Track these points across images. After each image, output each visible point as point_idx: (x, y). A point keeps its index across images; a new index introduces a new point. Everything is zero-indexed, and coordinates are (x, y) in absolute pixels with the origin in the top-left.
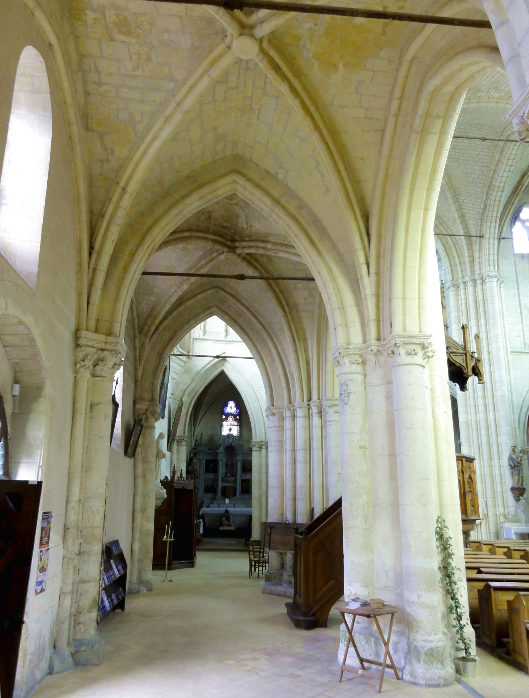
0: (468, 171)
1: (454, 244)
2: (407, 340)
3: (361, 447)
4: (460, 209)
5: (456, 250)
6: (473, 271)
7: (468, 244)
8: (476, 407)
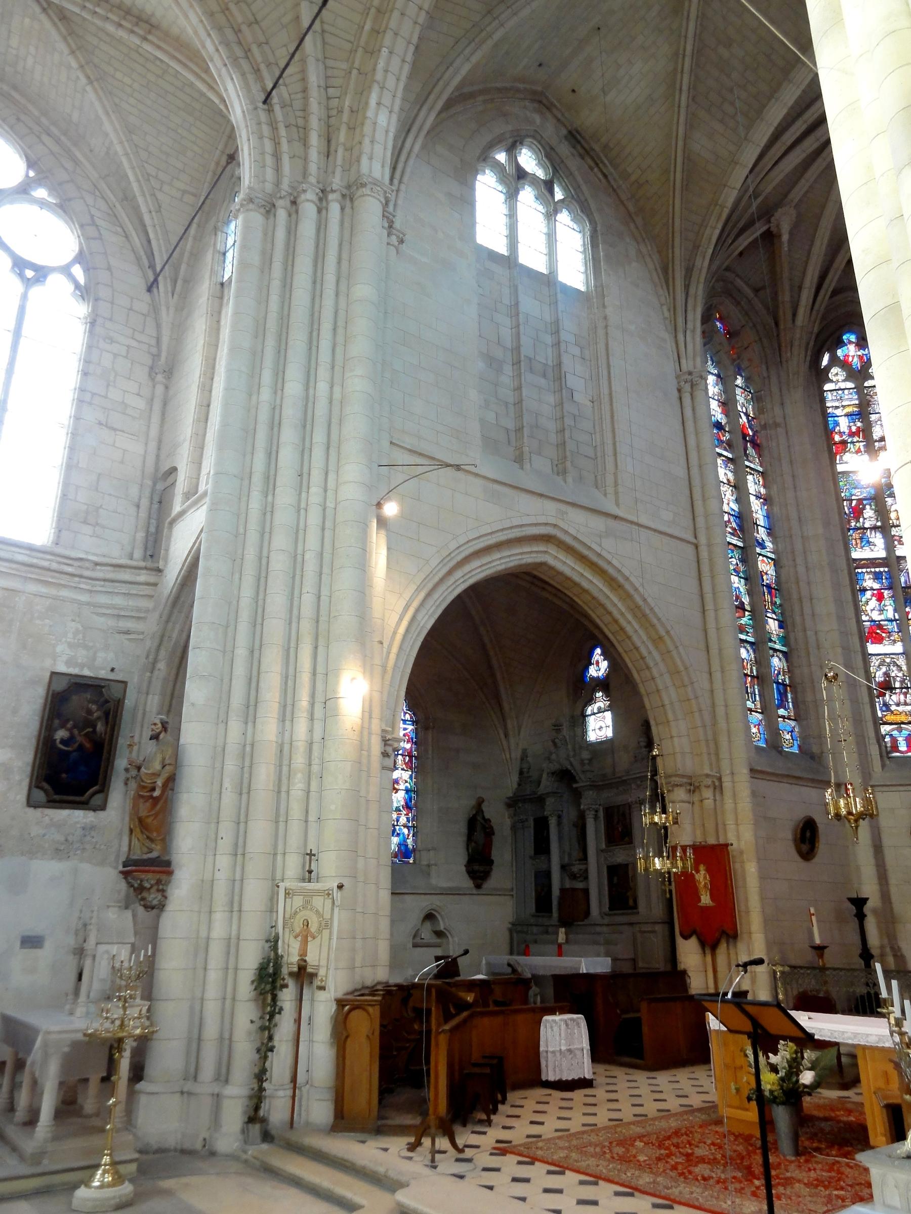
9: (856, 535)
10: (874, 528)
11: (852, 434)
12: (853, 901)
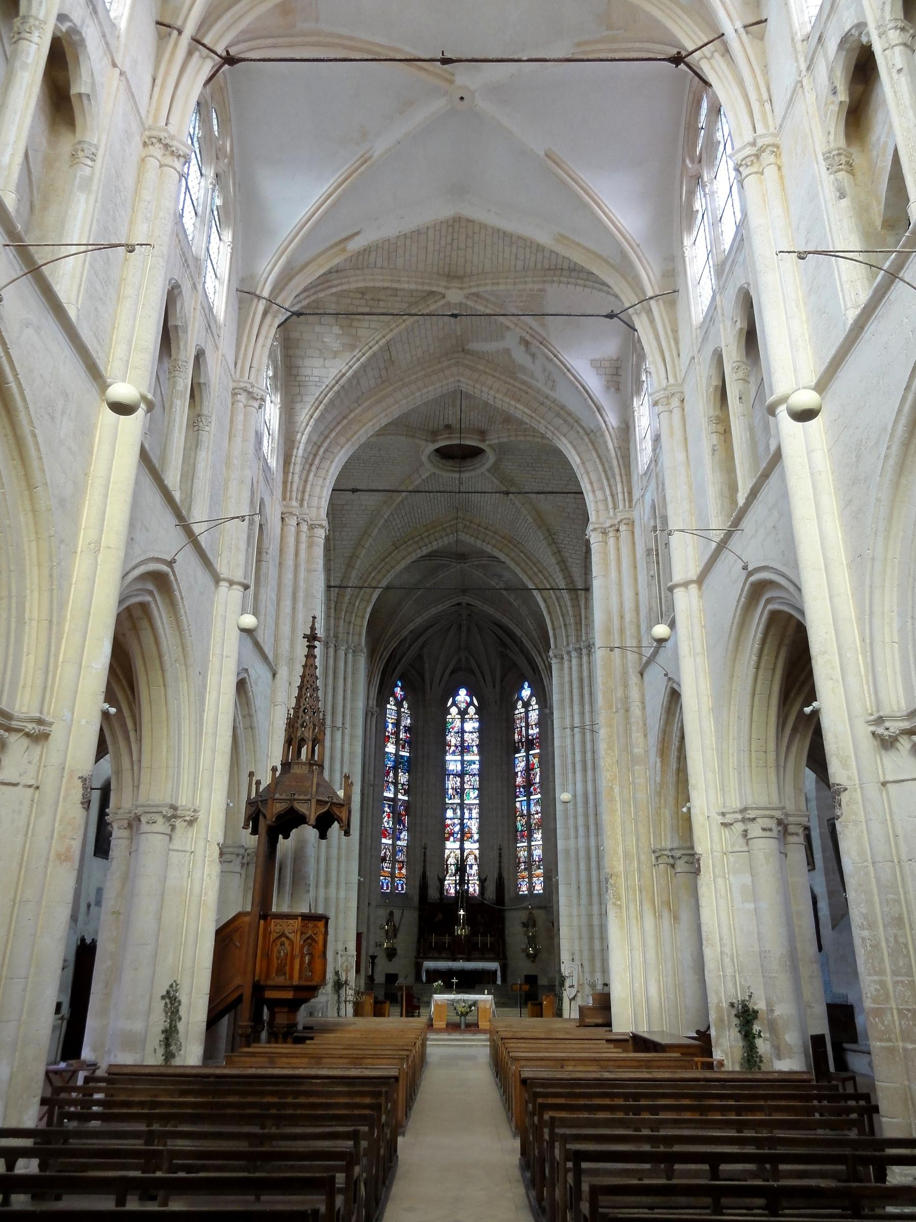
0: (559, 504)
2: (147, 809)
3: (113, 913)
4: (558, 552)
6: (578, 638)
7: (572, 599)
10: (392, 782)
11: (392, 734)
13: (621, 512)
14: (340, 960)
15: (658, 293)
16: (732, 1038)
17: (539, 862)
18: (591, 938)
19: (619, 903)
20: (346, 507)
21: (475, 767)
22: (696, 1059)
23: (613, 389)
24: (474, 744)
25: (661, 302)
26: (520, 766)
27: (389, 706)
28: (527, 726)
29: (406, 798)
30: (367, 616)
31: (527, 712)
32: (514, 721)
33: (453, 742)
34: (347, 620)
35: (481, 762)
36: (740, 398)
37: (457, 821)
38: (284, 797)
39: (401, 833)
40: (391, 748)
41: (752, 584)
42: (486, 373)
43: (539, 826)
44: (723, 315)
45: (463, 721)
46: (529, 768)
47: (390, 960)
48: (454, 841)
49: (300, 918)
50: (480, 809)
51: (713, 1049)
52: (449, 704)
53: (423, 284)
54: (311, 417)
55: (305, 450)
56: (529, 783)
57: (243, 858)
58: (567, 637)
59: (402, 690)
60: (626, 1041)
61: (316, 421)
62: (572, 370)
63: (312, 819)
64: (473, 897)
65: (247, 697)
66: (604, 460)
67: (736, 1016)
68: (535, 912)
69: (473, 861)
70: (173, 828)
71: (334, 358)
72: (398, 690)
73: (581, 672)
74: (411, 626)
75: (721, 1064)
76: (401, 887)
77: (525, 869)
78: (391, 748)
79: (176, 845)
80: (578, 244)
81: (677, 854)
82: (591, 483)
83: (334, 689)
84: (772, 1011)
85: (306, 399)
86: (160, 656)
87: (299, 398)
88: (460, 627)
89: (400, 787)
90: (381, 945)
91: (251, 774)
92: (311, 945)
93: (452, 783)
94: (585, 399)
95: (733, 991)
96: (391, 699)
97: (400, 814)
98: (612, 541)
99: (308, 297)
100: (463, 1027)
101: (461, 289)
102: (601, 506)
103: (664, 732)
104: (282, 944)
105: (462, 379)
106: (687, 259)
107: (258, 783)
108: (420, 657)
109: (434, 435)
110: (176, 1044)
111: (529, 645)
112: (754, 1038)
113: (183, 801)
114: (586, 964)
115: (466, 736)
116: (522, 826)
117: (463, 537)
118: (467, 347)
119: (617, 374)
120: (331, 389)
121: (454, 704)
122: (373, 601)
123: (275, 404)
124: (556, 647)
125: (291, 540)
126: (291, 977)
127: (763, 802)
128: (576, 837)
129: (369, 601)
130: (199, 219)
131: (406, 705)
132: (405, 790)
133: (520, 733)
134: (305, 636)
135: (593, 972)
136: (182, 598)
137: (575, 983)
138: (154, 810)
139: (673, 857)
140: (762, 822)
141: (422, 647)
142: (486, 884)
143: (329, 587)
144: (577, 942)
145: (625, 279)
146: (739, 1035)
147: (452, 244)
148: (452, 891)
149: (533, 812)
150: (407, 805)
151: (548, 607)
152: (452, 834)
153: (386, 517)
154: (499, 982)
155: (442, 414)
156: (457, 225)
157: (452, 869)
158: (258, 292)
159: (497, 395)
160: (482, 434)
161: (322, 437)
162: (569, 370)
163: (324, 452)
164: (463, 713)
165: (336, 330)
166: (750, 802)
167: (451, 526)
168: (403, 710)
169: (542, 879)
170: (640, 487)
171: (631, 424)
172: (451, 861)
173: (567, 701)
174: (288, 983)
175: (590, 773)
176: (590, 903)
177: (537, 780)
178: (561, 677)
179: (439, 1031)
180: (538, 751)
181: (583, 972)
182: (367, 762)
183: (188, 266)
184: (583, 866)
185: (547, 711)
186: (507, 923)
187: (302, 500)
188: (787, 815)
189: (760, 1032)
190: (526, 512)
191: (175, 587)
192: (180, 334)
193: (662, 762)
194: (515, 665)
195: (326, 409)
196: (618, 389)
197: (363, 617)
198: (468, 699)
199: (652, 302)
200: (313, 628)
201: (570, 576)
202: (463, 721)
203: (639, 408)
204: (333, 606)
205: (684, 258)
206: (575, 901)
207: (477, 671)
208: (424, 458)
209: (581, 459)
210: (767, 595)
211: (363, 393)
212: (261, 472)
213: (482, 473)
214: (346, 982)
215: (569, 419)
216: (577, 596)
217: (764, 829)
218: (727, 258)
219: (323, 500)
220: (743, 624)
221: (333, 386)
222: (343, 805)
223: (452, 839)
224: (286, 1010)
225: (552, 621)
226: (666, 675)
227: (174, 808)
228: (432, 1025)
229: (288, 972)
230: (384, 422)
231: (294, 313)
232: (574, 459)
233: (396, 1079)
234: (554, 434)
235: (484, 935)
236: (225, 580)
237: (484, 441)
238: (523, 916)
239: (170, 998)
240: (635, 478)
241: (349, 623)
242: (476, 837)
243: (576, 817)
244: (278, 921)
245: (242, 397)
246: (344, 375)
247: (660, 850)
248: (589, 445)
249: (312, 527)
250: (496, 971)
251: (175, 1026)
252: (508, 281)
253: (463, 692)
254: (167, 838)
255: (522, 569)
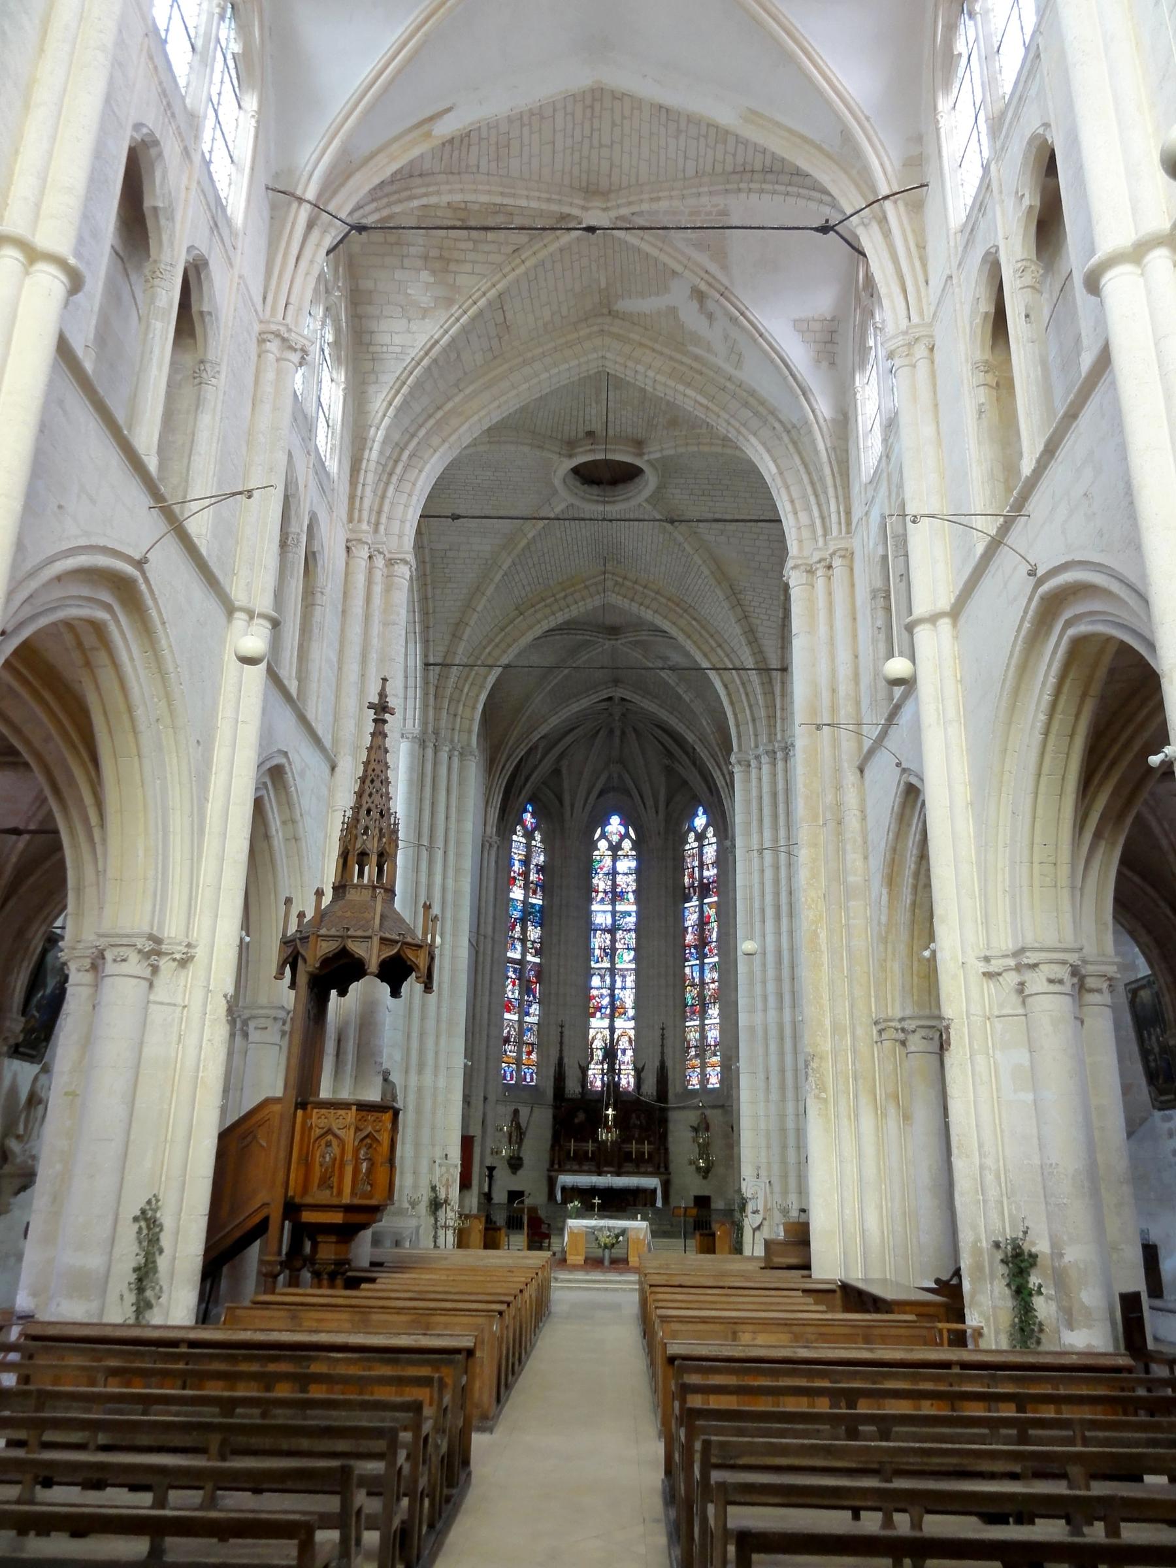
0: (747, 549)
1: (743, 684)
3: (66, 1094)
5: (747, 695)
7: (763, 684)
8: (765, 998)
9: (510, 941)
10: (519, 939)
11: (519, 874)
12: (488, 1168)
13: (836, 538)
14: (438, 1171)
15: (896, 189)
16: (996, 1293)
17: (715, 1046)
18: (784, 1147)
19: (823, 1095)
20: (449, 554)
21: (631, 921)
22: (940, 1325)
23: (825, 364)
24: (630, 889)
25: (900, 204)
26: (691, 919)
27: (515, 838)
28: (701, 866)
29: (537, 960)
30: (480, 707)
31: (701, 847)
32: (683, 859)
33: (602, 887)
34: (452, 712)
35: (638, 913)
36: (1027, 316)
37: (605, 992)
38: (333, 932)
39: (530, 1006)
40: (517, 893)
41: (1042, 598)
42: (641, 345)
43: (715, 999)
44: (1001, 192)
45: (615, 858)
46: (703, 922)
47: (514, 1173)
48: (602, 1018)
49: (354, 1108)
50: (637, 975)
51: (967, 1311)
52: (597, 836)
53: (549, 200)
54: (390, 404)
55: (381, 452)
56: (703, 942)
57: (284, 1024)
58: (756, 735)
59: (533, 816)
60: (833, 1291)
61: (399, 410)
62: (766, 334)
63: (373, 965)
64: (627, 1093)
65: (287, 793)
66: (812, 468)
67: (1002, 1261)
68: (708, 1112)
69: (627, 1045)
70: (155, 970)
71: (423, 318)
72: (528, 818)
73: (774, 783)
74: (544, 729)
75: (978, 1333)
76: (530, 1077)
77: (697, 1056)
78: (517, 893)
79: (160, 994)
80: (778, 124)
81: (910, 1025)
82: (792, 502)
83: (433, 804)
84: (1061, 1255)
85: (383, 378)
86: (130, 709)
87: (373, 377)
88: (611, 732)
89: (529, 945)
90: (498, 1152)
91: (288, 901)
92: (370, 1146)
93: (599, 941)
94: (785, 378)
95: (998, 1224)
96: (518, 828)
97: (529, 981)
98: (820, 583)
99: (377, 210)
100: (607, 1263)
101: (605, 209)
102: (806, 534)
103: (894, 850)
104: (329, 1144)
105: (608, 355)
106: (942, 131)
107: (301, 915)
108: (557, 772)
109: (571, 446)
110: (153, 1289)
111: (704, 754)
112: (1030, 1295)
113: (172, 930)
114: (775, 1181)
115: (620, 879)
116: (693, 998)
117: (615, 599)
118: (615, 308)
119: (831, 342)
120: (419, 364)
121: (603, 836)
122: (489, 686)
123: (337, 384)
124: (740, 746)
125: (360, 579)
126: (340, 1193)
127: (1051, 940)
128: (765, 1010)
129: (482, 687)
130: (198, 57)
131: (538, 836)
132: (536, 949)
133: (691, 876)
134: (371, 706)
135: (785, 1193)
136: (164, 623)
137: (761, 1208)
138: (124, 941)
139: (903, 1030)
140: (1046, 970)
141: (561, 756)
142: (643, 1075)
143: (427, 665)
144: (763, 1153)
145: (846, 172)
146: (1007, 1291)
147: (591, 137)
148: (598, 1083)
149: (707, 980)
150: (539, 970)
151: (729, 695)
152: (599, 1009)
153: (505, 567)
154: (659, 1204)
155: (581, 413)
156: (597, 106)
157: (599, 1055)
158: (299, 193)
159: (658, 377)
160: (639, 445)
161: (407, 436)
162: (761, 335)
163: (410, 457)
164: (615, 848)
165: (425, 276)
166: (1029, 940)
167: (596, 584)
168: (534, 843)
169: (718, 1069)
170: (864, 502)
171: (850, 414)
172: (598, 1044)
173: (755, 823)
174: (335, 1201)
175: (785, 921)
176: (783, 1098)
177: (714, 936)
178: (747, 791)
179: (575, 1268)
180: (715, 899)
181: (772, 1193)
182: (483, 911)
183: (173, 115)
184: (773, 1047)
185: (728, 843)
186: (671, 1126)
187: (377, 524)
188: (1085, 962)
189: (1040, 1286)
190: (700, 562)
191: (150, 603)
192: (163, 222)
193: (889, 894)
194: (685, 783)
195: (410, 393)
196: (833, 364)
197: (474, 708)
198: (622, 830)
199: (888, 204)
200: (382, 694)
201: (761, 652)
202: (615, 858)
203: (863, 388)
204: (432, 691)
205: (938, 130)
206: (761, 1096)
207: (635, 792)
208: (557, 482)
209: (777, 466)
210: (1067, 614)
211: (465, 374)
212: (311, 471)
213: (640, 505)
214: (446, 1201)
215: (761, 409)
216: (771, 679)
217: (1051, 981)
218: (1007, 106)
219: (408, 525)
220: (1024, 667)
221: (422, 359)
222: (420, 947)
223: (598, 1015)
224: (333, 1239)
225: (735, 715)
226: (898, 765)
227: (158, 941)
228: (565, 1260)
229: (335, 1185)
230: (496, 417)
231: (353, 227)
232: (768, 468)
233: (470, 1353)
234: (739, 432)
235: (640, 1141)
236: (241, 609)
237: (641, 455)
238: (692, 1117)
239: (146, 1220)
240: (855, 489)
241: (455, 715)
242: (631, 1013)
243: (764, 982)
244: (323, 1111)
245: (273, 346)
246: (437, 342)
247: (886, 1020)
248: (790, 447)
249: (390, 563)
250: (654, 1191)
251: (154, 1262)
252: (674, 193)
253: (615, 820)
254: (145, 984)
255: (695, 642)
